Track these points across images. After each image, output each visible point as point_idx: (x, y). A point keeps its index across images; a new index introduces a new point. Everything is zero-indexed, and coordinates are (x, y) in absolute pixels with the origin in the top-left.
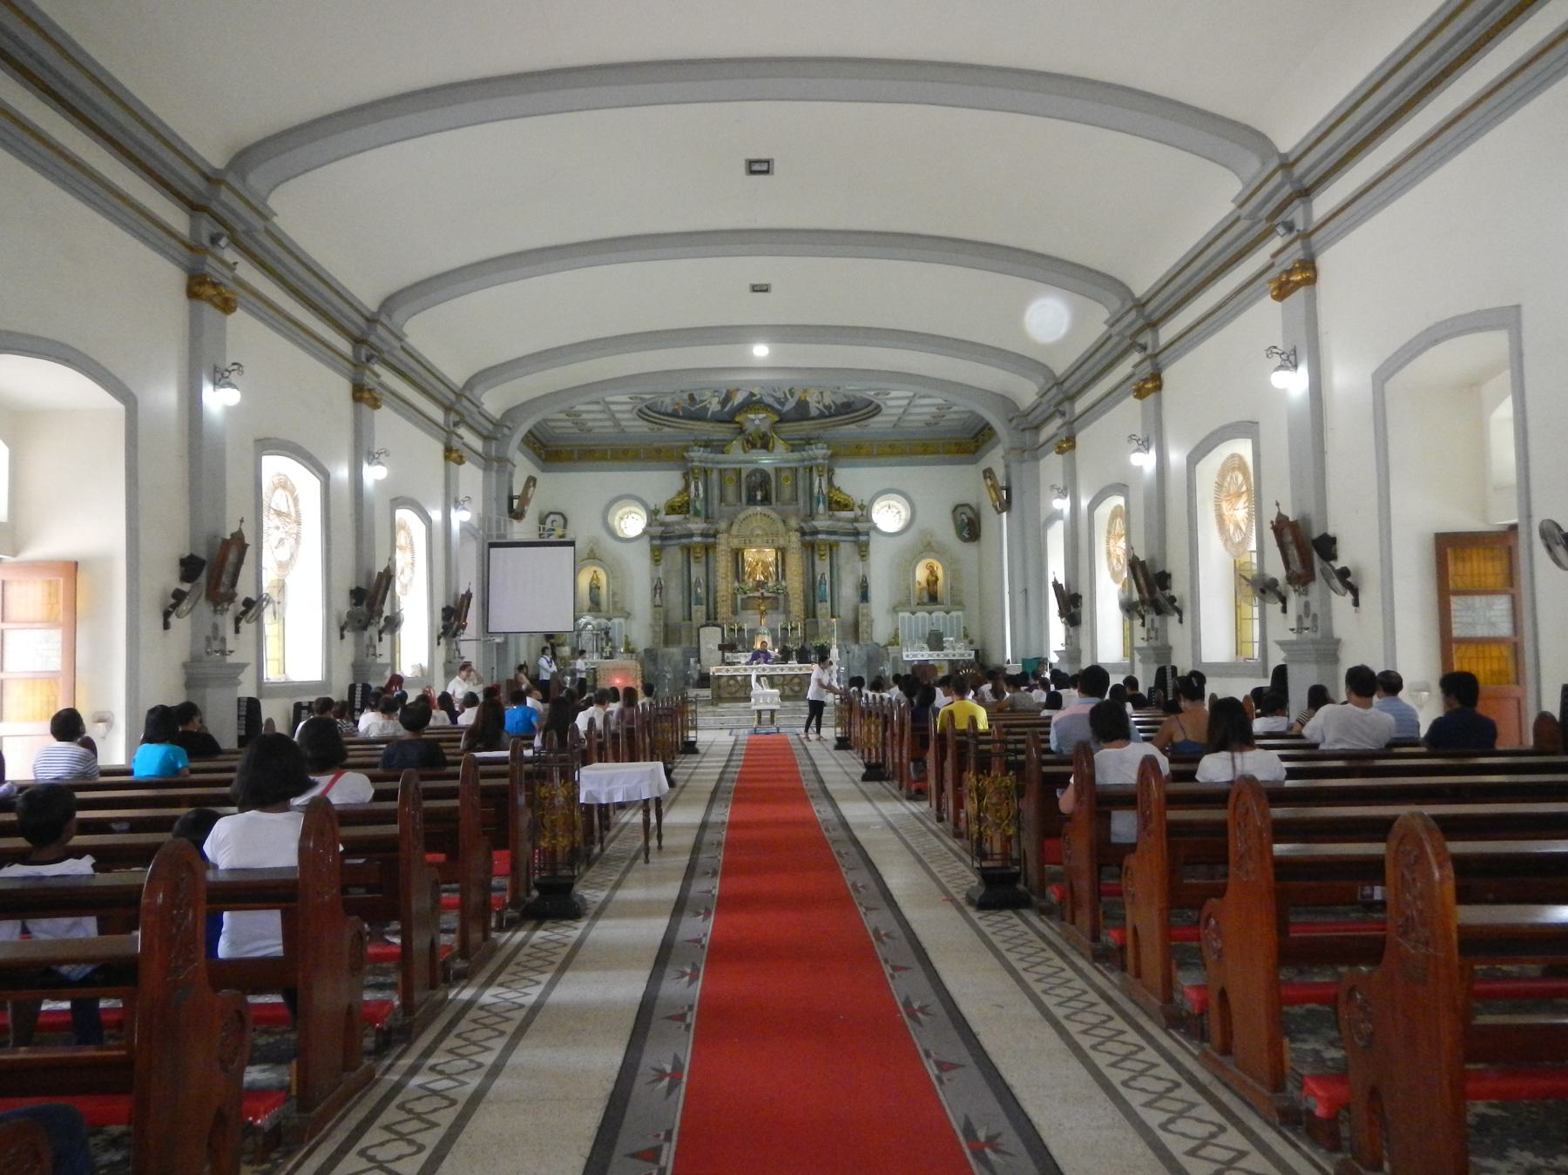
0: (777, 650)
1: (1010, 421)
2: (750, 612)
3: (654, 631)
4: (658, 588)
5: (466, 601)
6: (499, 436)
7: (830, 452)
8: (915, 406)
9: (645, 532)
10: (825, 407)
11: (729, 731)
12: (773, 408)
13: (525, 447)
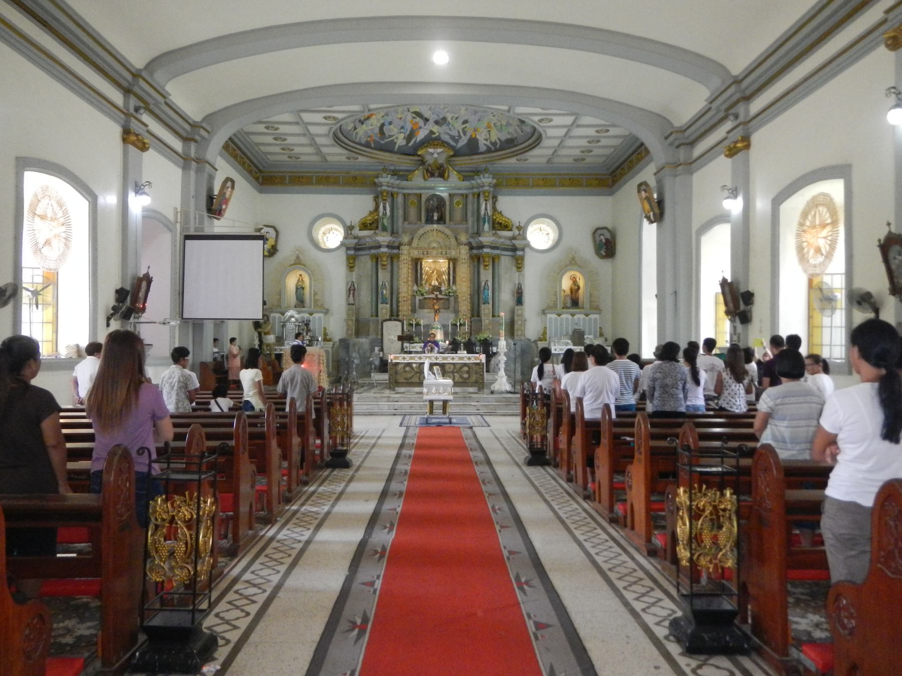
0: (447, 342)
1: (666, 138)
2: (426, 311)
3: (348, 325)
4: (352, 290)
5: (144, 284)
6: (197, 137)
7: (495, 181)
8: (571, 137)
9: (342, 244)
10: (491, 142)
11: (399, 419)
12: (448, 144)
13: (226, 154)
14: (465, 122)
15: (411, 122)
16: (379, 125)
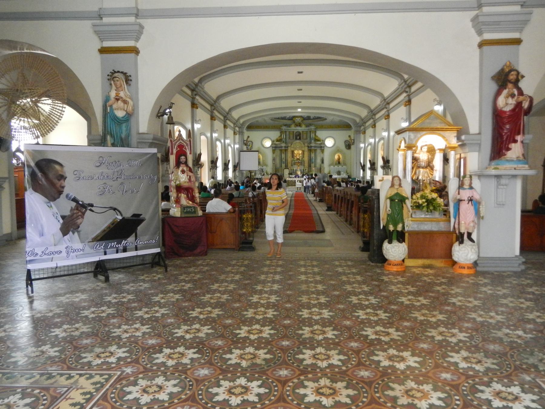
4: (274, 159)
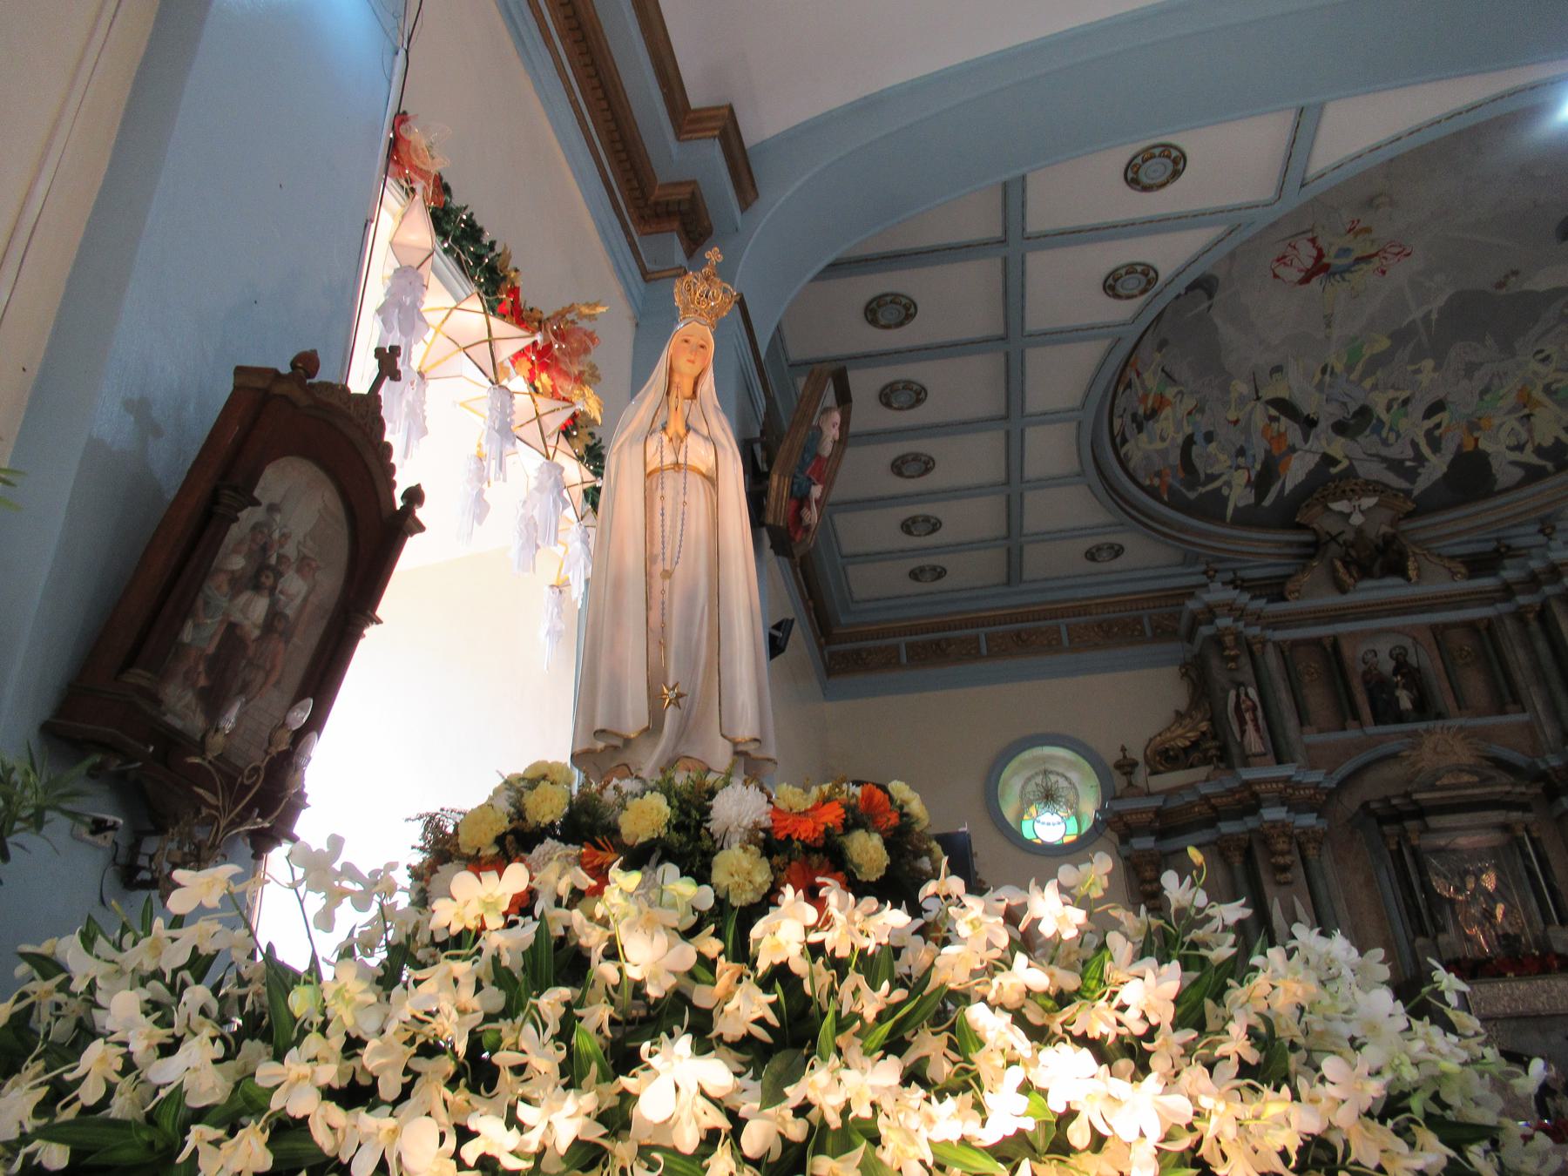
10: (1540, 451)
14: (1437, 407)
15: (1264, 433)
16: (1180, 440)
